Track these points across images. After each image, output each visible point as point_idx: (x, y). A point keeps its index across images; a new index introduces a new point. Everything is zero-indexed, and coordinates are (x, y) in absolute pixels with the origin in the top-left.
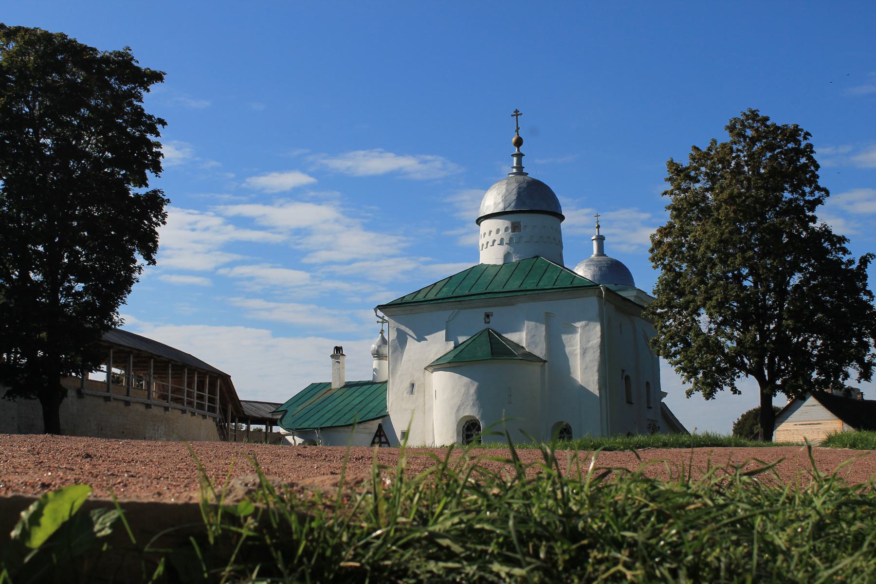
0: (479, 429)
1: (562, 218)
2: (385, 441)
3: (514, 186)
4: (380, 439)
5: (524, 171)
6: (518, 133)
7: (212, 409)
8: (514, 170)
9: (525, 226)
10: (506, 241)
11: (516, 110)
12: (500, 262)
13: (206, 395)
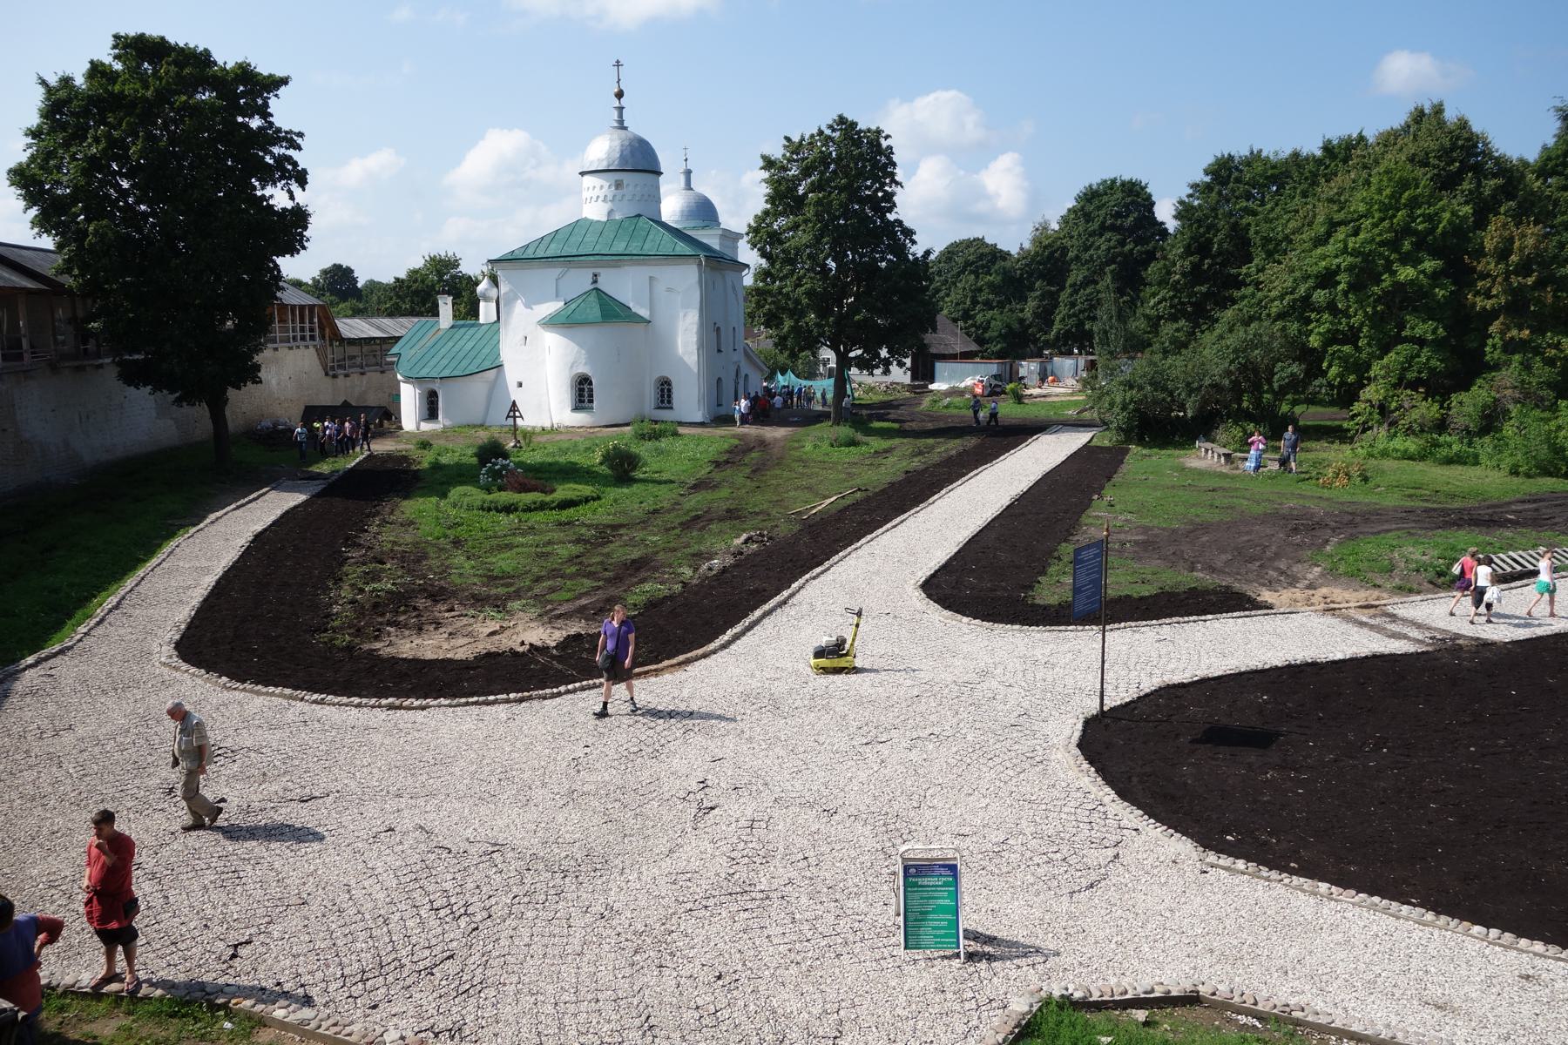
0: (591, 383)
1: (660, 173)
3: (617, 143)
7: (312, 338)
8: (616, 125)
9: (628, 185)
12: (604, 219)
13: (307, 325)
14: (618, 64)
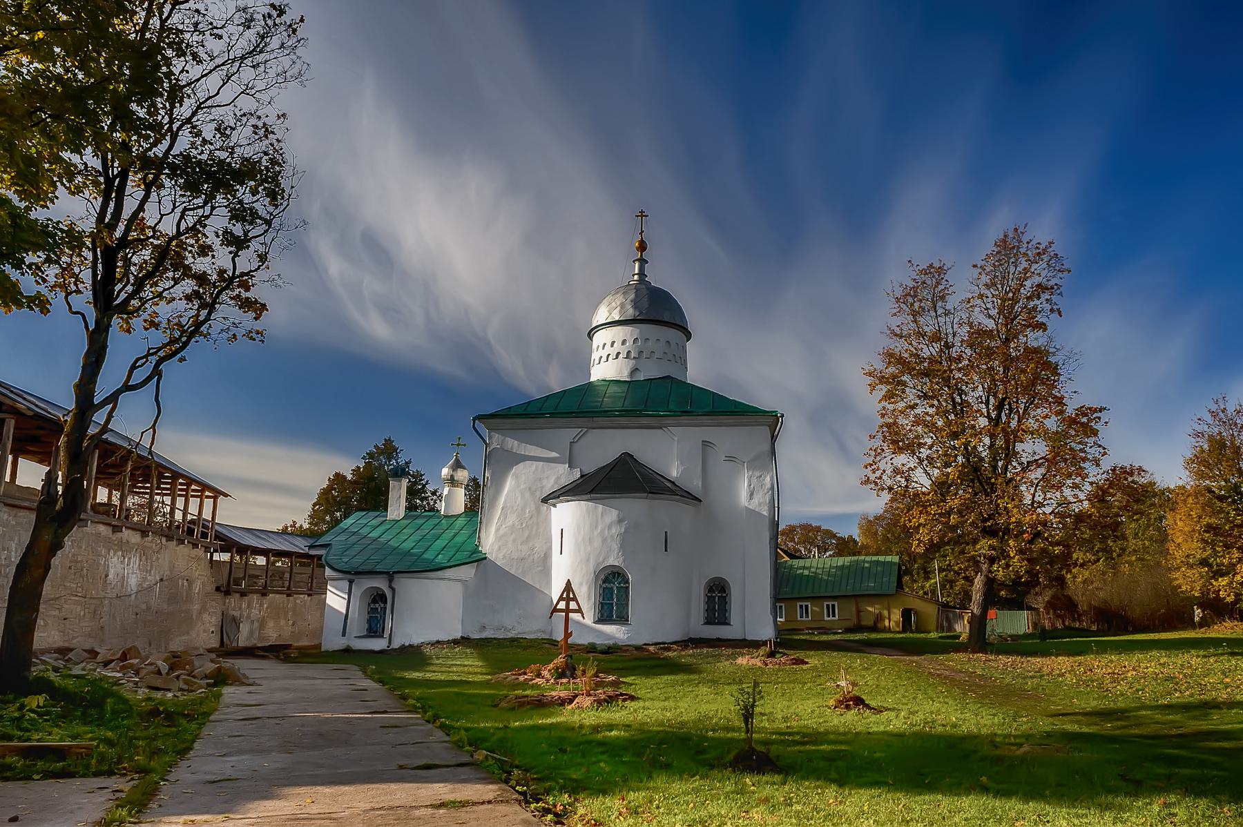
4: (568, 605)
14: (642, 215)
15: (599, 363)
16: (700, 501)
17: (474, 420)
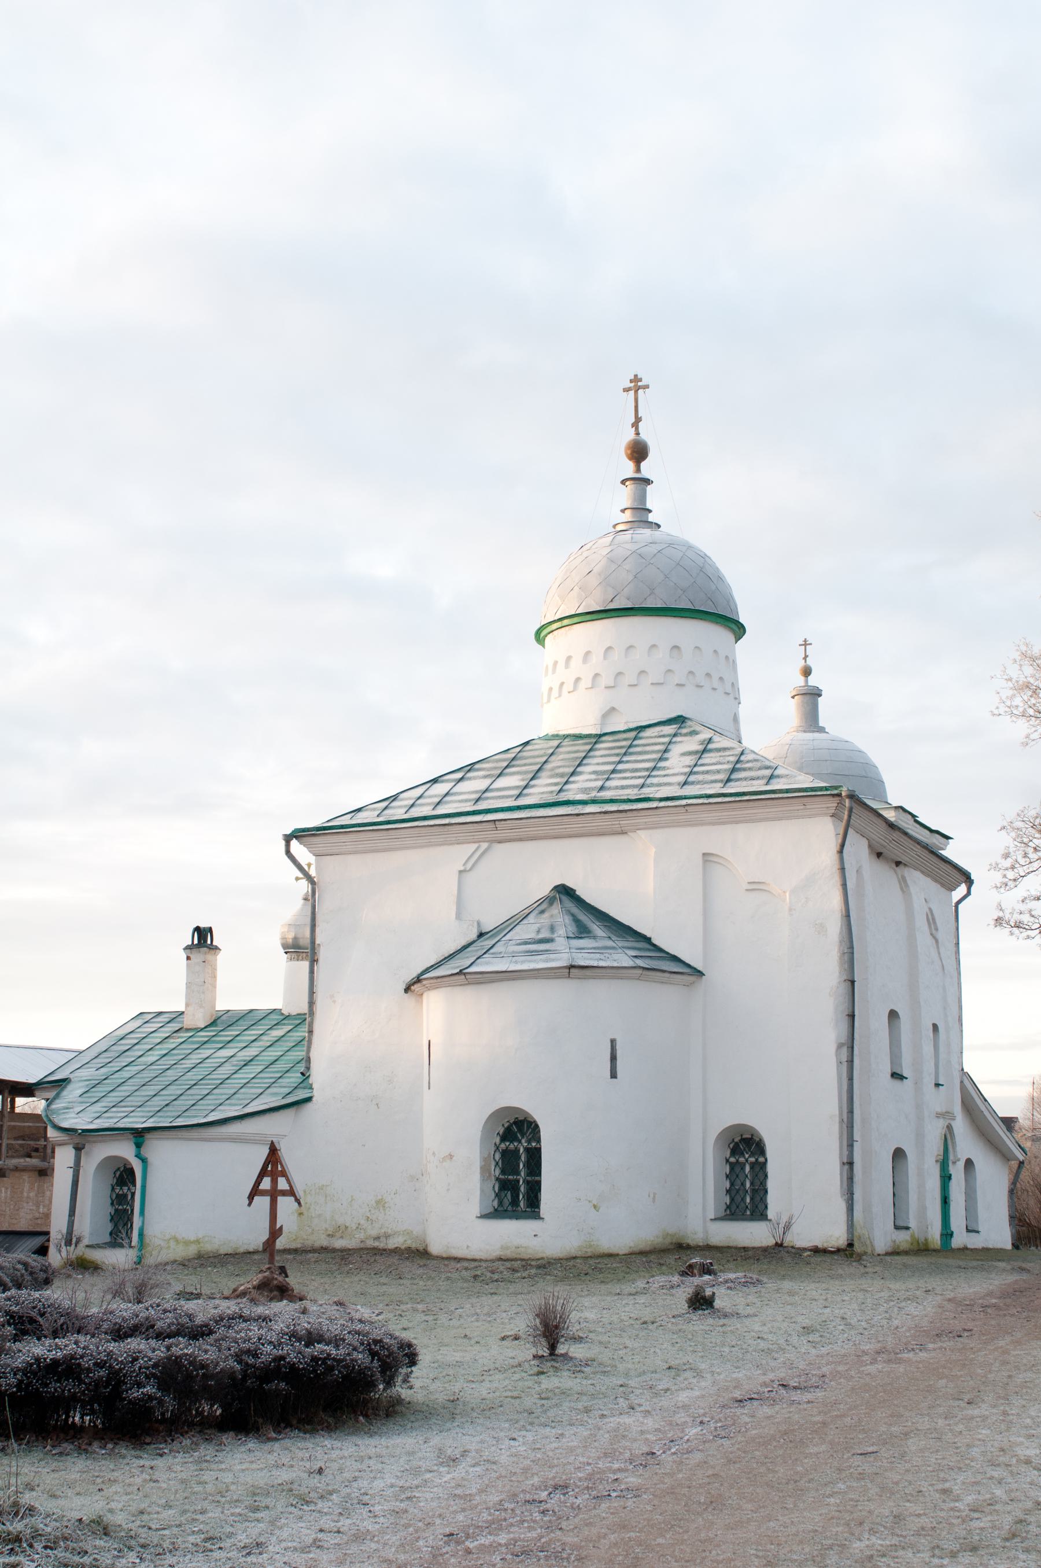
1: (738, 630)
2: (286, 1187)
4: (274, 1182)
5: (651, 518)
6: (637, 429)
10: (606, 680)
11: (636, 376)
15: (560, 696)
16: (700, 974)
17: (288, 839)
